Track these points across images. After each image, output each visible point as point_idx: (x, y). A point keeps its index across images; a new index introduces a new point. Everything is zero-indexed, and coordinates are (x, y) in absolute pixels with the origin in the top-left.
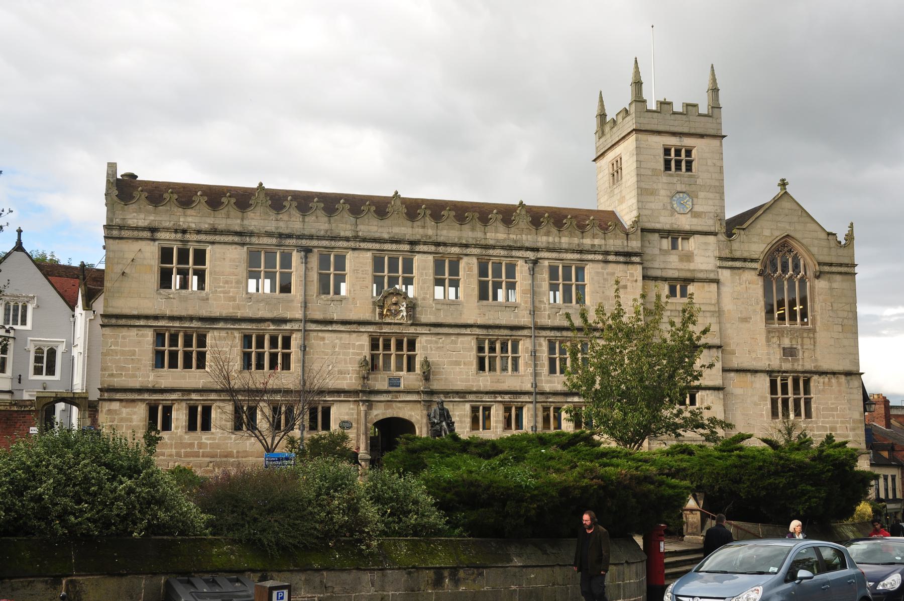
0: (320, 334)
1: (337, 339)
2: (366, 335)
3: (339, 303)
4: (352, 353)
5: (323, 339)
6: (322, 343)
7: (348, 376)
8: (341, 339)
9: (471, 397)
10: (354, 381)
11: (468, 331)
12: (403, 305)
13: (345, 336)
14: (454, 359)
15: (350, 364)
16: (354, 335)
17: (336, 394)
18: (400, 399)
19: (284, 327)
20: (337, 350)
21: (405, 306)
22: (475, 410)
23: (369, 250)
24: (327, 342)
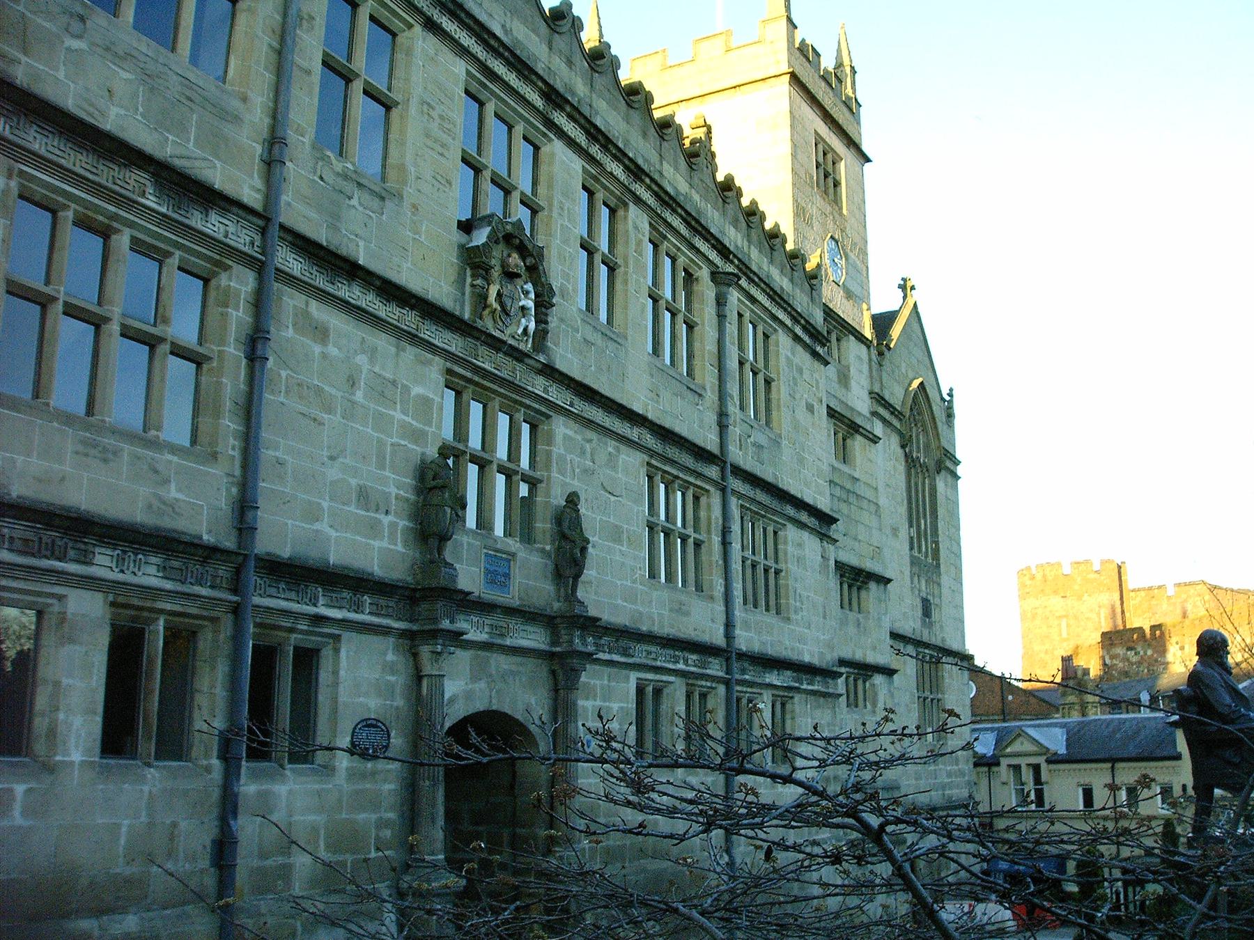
0: (316, 309)
1: (364, 352)
2: (438, 363)
3: (376, 203)
4: (403, 425)
5: (321, 333)
6: (317, 349)
7: (386, 520)
8: (373, 353)
9: (641, 654)
10: (400, 548)
11: (634, 433)
12: (526, 293)
13: (382, 341)
14: (612, 520)
15: (394, 469)
16: (411, 352)
17: (346, 594)
18: (508, 642)
19: (196, 220)
20: (359, 396)
21: (532, 296)
22: (640, 691)
23: (464, 52)
24: (333, 350)
